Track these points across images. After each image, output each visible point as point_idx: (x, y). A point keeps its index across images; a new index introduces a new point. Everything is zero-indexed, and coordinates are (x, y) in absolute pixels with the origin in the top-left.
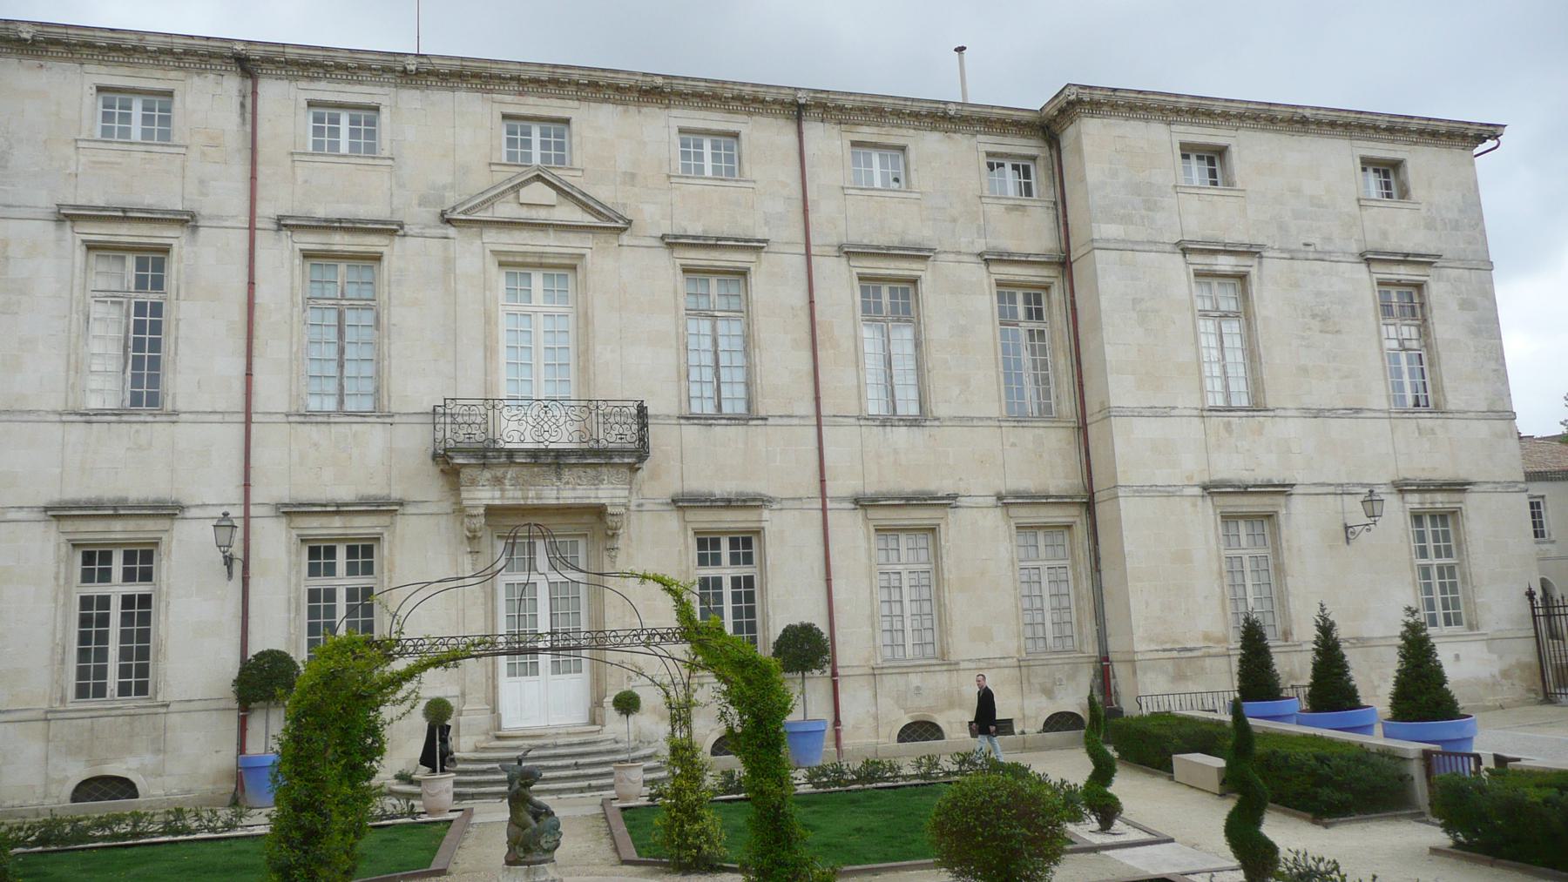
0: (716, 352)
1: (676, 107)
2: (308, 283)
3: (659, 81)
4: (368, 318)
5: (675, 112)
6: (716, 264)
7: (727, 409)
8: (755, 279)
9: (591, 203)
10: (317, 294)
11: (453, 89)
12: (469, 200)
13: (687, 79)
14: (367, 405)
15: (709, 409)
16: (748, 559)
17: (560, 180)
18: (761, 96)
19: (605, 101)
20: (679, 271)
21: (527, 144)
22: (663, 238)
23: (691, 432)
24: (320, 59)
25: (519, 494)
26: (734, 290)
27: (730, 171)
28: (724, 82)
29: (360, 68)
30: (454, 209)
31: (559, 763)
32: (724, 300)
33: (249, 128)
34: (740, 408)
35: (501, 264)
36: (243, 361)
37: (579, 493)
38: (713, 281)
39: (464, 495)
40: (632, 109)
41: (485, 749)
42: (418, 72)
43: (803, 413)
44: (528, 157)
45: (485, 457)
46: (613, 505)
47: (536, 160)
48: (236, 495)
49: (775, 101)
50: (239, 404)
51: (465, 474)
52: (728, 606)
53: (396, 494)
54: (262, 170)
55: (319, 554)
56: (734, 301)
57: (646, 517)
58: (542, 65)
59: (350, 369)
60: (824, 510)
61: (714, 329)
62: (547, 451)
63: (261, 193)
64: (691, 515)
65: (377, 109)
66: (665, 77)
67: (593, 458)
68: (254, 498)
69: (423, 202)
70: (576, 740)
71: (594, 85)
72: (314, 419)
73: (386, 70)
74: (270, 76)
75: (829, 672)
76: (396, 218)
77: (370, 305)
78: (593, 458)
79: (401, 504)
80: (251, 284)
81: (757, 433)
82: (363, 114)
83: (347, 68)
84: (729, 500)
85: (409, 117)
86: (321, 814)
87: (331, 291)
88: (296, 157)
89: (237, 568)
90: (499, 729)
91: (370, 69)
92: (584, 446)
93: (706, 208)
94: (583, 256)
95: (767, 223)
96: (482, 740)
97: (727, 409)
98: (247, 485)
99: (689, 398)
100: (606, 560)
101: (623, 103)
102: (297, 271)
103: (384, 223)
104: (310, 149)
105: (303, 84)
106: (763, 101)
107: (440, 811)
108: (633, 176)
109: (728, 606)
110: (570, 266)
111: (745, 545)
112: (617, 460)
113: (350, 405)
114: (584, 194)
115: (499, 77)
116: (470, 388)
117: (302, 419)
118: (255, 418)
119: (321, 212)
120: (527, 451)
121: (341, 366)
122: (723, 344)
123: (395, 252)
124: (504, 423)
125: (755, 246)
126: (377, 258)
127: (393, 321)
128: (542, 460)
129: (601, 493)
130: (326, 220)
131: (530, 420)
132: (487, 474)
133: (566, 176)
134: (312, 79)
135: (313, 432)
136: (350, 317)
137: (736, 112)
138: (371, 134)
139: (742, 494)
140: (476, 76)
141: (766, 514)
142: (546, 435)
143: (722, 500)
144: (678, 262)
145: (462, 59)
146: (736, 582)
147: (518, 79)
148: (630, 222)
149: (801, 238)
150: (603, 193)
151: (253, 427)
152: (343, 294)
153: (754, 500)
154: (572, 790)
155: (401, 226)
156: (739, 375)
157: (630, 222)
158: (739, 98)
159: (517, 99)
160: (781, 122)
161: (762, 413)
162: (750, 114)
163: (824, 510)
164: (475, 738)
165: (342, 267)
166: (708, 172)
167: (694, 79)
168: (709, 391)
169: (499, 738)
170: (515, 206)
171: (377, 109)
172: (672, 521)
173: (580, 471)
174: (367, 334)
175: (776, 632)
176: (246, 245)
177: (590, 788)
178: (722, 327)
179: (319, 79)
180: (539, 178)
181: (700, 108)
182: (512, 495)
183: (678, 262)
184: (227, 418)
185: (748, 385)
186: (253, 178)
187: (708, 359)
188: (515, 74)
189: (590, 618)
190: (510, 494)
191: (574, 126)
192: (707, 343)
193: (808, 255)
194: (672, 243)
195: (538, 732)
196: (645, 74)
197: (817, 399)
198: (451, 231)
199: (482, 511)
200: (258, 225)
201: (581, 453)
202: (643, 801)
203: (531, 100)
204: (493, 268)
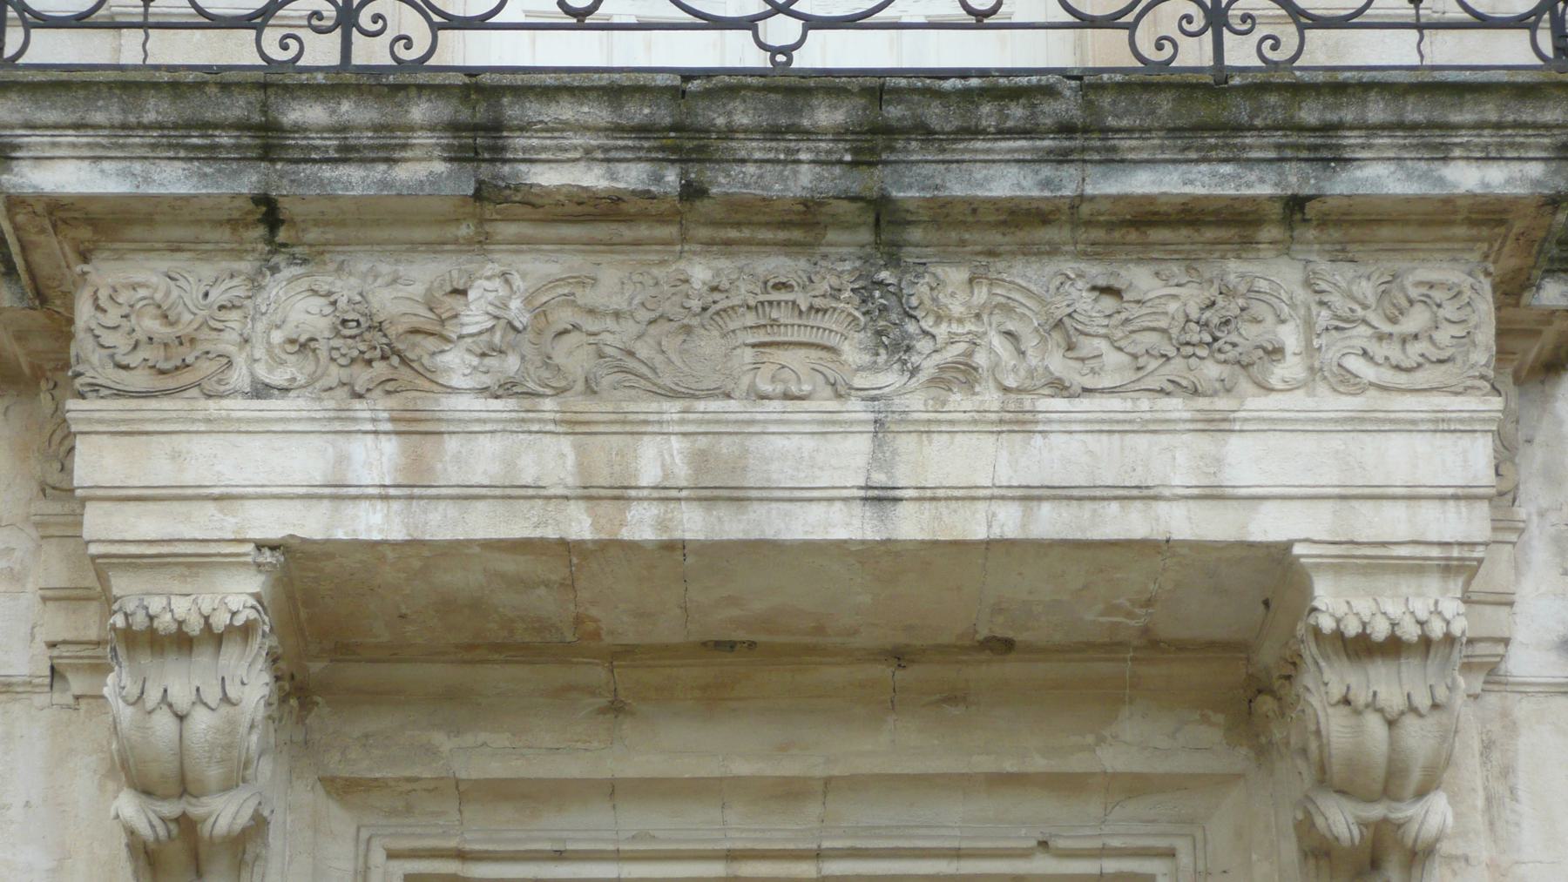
25: (551, 459)
37: (1058, 455)
39: (95, 463)
46: (1370, 562)
51: (119, 298)
62: (786, 90)
92: (1106, 51)
112: (1380, 176)
120: (614, 88)
128: (747, 176)
129: (1245, 461)
132: (296, 303)
173: (1055, 281)
182: (494, 472)
190: (478, 458)
199: (237, 595)
201: (1073, 115)
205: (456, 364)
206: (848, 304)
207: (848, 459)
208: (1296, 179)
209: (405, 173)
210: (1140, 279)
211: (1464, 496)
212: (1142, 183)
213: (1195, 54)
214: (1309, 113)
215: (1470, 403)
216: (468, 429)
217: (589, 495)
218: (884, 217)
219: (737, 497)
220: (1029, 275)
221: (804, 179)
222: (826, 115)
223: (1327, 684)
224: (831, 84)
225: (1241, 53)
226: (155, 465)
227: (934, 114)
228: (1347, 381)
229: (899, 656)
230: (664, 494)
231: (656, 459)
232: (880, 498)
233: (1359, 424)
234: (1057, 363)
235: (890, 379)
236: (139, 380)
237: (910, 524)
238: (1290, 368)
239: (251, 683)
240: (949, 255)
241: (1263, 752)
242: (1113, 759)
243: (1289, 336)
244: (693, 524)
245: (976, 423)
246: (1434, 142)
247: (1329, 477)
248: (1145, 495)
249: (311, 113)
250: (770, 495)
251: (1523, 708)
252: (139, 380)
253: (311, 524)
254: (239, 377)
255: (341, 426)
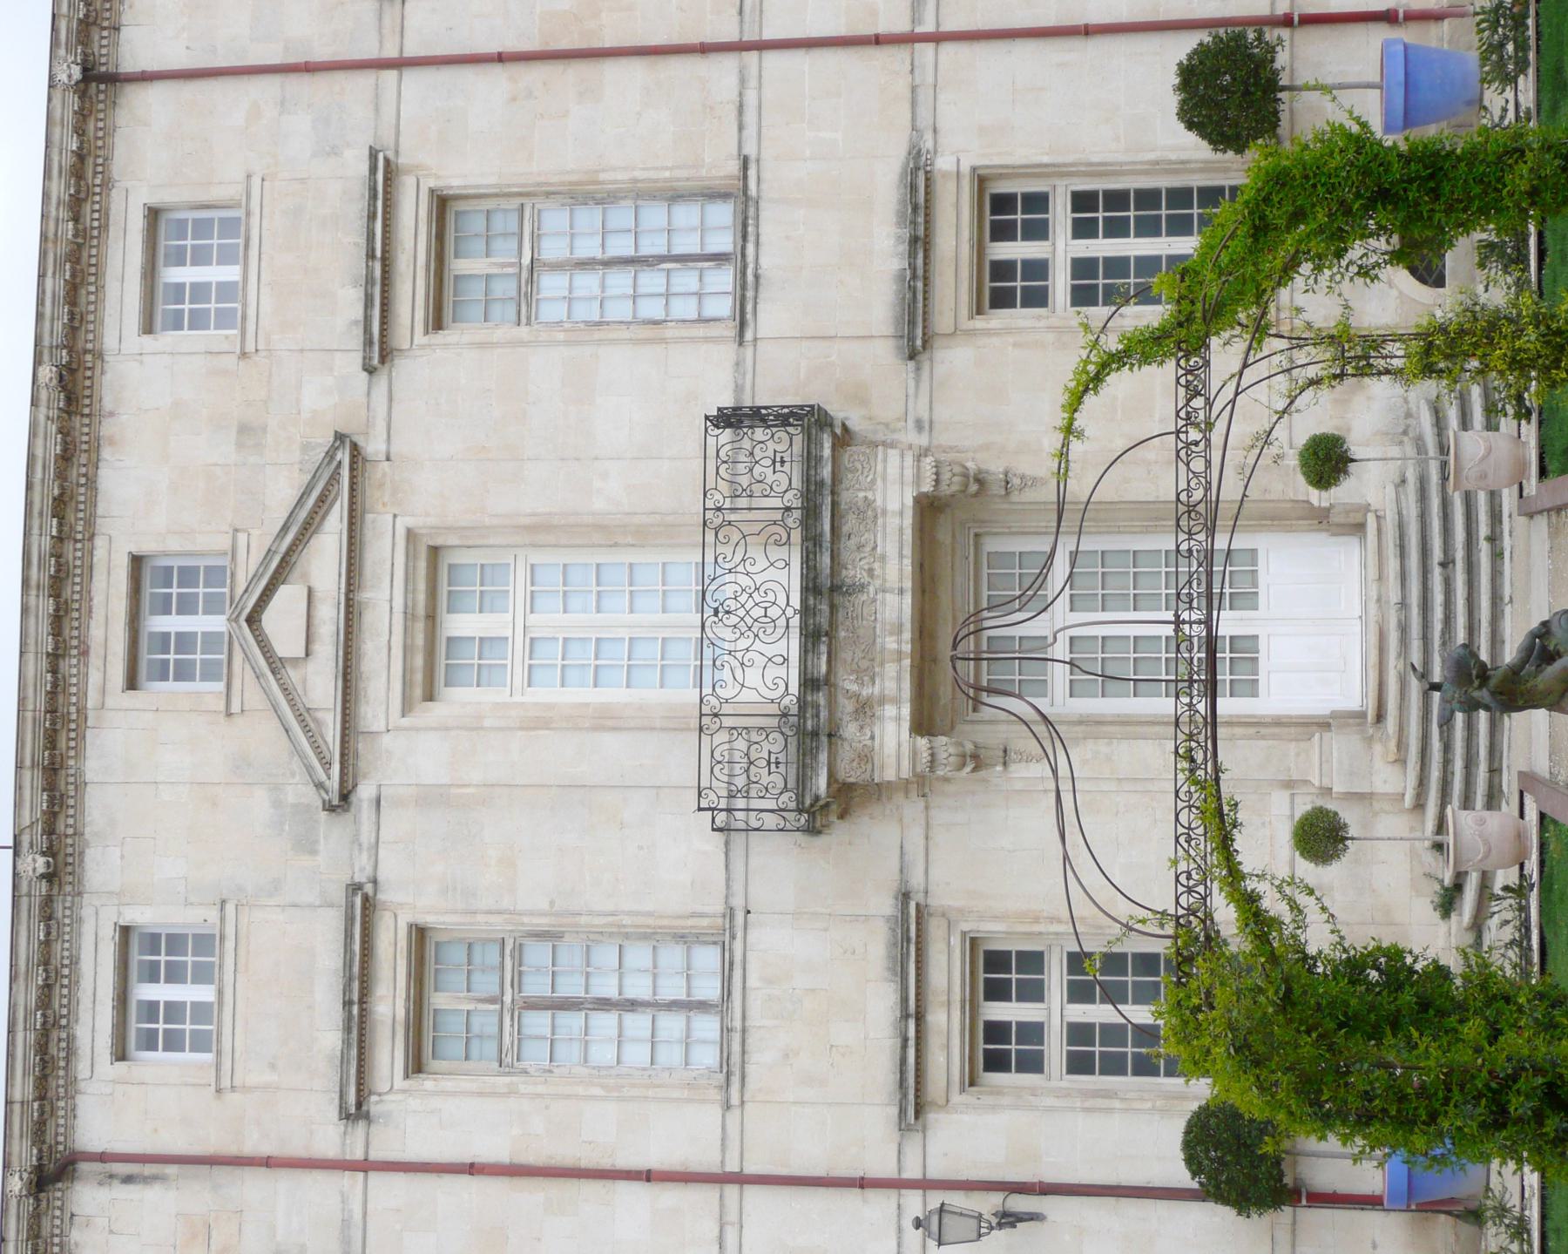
0: (608, 263)
1: (98, 338)
2: (470, 1065)
3: (47, 372)
4: (538, 954)
5: (110, 341)
6: (423, 260)
7: (723, 242)
8: (456, 175)
9: (303, 515)
10: (491, 1048)
11: (80, 786)
12: (302, 756)
13: (39, 316)
14: (708, 958)
15: (723, 279)
16: (1037, 202)
17: (256, 576)
18: (68, 160)
19: (91, 483)
20: (439, 337)
21: (185, 641)
22: (370, 370)
23: (770, 318)
24: (32, 1037)
25: (891, 669)
26: (477, 224)
27: (230, 227)
28: (44, 237)
29: (46, 963)
30: (319, 786)
31: (1438, 598)
32: (498, 244)
33: (171, 1170)
34: (723, 214)
35: (430, 696)
36: (622, 1186)
38: (459, 266)
39: (890, 775)
40: (107, 428)
41: (1401, 745)
42: (50, 852)
43: (732, 81)
44: (211, 640)
45: (815, 734)
47: (216, 623)
48: (880, 1205)
49: (80, 131)
50: (706, 1196)
51: (849, 771)
52: (1134, 247)
53: (886, 905)
54: (253, 1144)
55: (1000, 1051)
56: (499, 223)
57: (943, 413)
58: (25, 610)
59: (638, 988)
60: (938, 38)
61: (557, 267)
62: (806, 611)
63: (296, 1147)
64: (943, 320)
65: (125, 931)
66: (38, 362)
67: (820, 519)
68: (887, 1170)
69: (307, 846)
70: (1393, 565)
71: (60, 505)
72: (736, 1058)
73: (48, 917)
74: (70, 1128)
75: (1285, 33)
76: (340, 896)
77: (513, 949)
78: (820, 519)
79: (905, 896)
80: (472, 1169)
81: (772, 181)
82: (137, 957)
83: (47, 987)
84: (914, 240)
85: (141, 866)
86: (1514, 1078)
87: (485, 1021)
88: (226, 1083)
89: (1020, 1203)
90: (1362, 715)
91: (47, 943)
92: (796, 536)
93: (306, 278)
94: (410, 535)
95: (334, 152)
96: (1383, 751)
97: (723, 242)
98: (863, 1183)
99: (702, 320)
100: (1029, 495)
101: (95, 447)
102: (448, 1084)
103: (349, 920)
104: (209, 1057)
105: (82, 1068)
106: (81, 156)
107: (1520, 837)
108: (244, 429)
109: (1134, 247)
110: (432, 560)
111: (1006, 209)
112: (826, 472)
113: (709, 989)
114: (285, 529)
115: (53, 694)
116: (679, 761)
117: (736, 1080)
118: (732, 1166)
119: (330, 1038)
121: (632, 1005)
122: (588, 248)
123: (409, 899)
124: (747, 695)
125: (384, 177)
126: (420, 934)
127: (545, 906)
129: (894, 505)
130: (347, 1029)
131: (743, 644)
132: (850, 730)
133: (248, 568)
134: (71, 1052)
135: (762, 1060)
136: (537, 986)
137: (105, 214)
138: (176, 942)
139: (901, 215)
140: (51, 740)
141: (944, 164)
142: (774, 612)
143: (912, 255)
144: (419, 338)
145: (19, 766)
146: (1083, 229)
147: (55, 658)
148: (340, 437)
149: (363, 82)
150: (282, 491)
151: (751, 1168)
152: (492, 1001)
153: (913, 188)
154: (1496, 574)
155: (355, 888)
156: (655, 215)
157: (340, 437)
158: (76, 205)
159: (95, 660)
160: (122, 117)
161: (733, 167)
162: (107, 184)
163: (938, 38)
164: (1379, 764)
165: (438, 1000)
166: (231, 273)
167: (40, 302)
168: (686, 279)
169: (1380, 717)
170: (311, 667)
171: (125, 931)
172: (954, 359)
173: (848, 547)
174: (570, 955)
175: (1193, 146)
176: (399, 1180)
177: (1493, 539)
178: (553, 249)
179: (71, 1039)
180: (253, 620)
181: (100, 288)
182: (893, 682)
183: (419, 338)
184: (732, 1216)
185: (675, 196)
186: (268, 1162)
187: (620, 281)
188: (44, 664)
189: (1146, 531)
190: (890, 686)
191: (145, 547)
192: (588, 282)
193: (400, 64)
194: (380, 351)
195: (1373, 639)
196: (34, 402)
197: (704, 49)
198: (365, 792)
199: (922, 742)
200: (359, 1155)
201: (812, 542)
202: (1530, 431)
203: (96, 633)
204: (436, 712)
205: (866, 692)
206: (852, 599)
207: (892, 599)
208: (827, 492)
209: (822, 702)
210: (845, 529)
211: (902, 456)
212: (827, 527)
213: (797, 514)
214: (813, 488)
215: (880, 456)
216: (882, 690)
217: (900, 660)
218: (834, 589)
219: (901, 625)
220: (845, 556)
221: (825, 607)
222: (811, 602)
223: (945, 490)
224: (804, 601)
225: (797, 503)
226: (891, 762)
227: (811, 575)
228: (873, 481)
229: (923, 592)
230: (899, 642)
231: (891, 643)
232: (901, 591)
233: (884, 479)
234: (868, 549)
235: (871, 589)
236: (869, 766)
237: (908, 584)
238: (870, 495)
239: (943, 739)
240: (839, 574)
241: (947, 505)
242: (948, 541)
243: (861, 494)
244: (907, 635)
245: (883, 568)
246: (819, 459)
247: (897, 487)
248: (901, 529)
249: (809, 723)
250: (900, 618)
251: (935, 442)
252: (869, 766)
253: (906, 725)
254: (869, 743)
255: (882, 719)
